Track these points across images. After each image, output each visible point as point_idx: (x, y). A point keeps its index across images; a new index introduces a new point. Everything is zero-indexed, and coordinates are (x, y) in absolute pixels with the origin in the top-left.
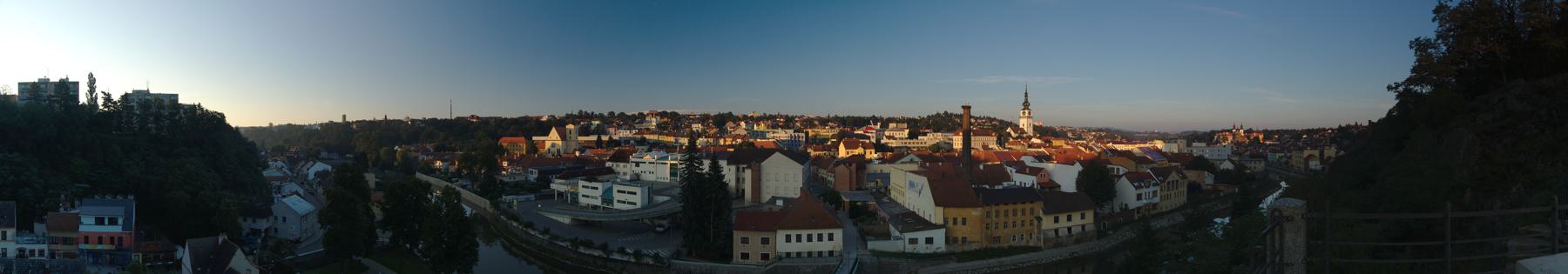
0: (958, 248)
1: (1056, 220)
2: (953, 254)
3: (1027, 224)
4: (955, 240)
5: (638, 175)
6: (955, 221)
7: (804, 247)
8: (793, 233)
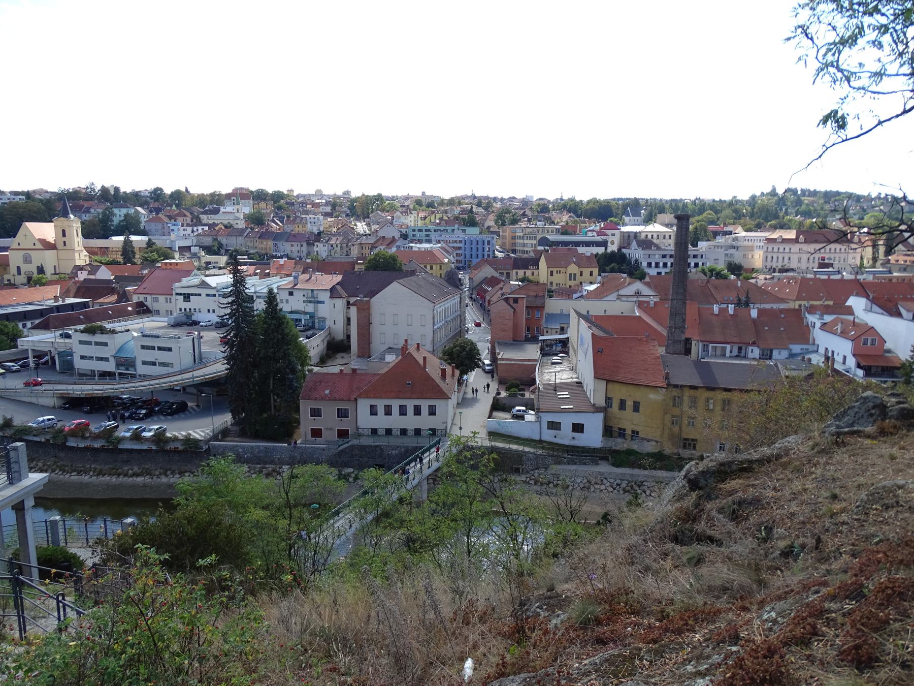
0: (621, 445)
4: (622, 433)
5: (188, 314)
6: (622, 405)
7: (396, 422)
8: (381, 404)
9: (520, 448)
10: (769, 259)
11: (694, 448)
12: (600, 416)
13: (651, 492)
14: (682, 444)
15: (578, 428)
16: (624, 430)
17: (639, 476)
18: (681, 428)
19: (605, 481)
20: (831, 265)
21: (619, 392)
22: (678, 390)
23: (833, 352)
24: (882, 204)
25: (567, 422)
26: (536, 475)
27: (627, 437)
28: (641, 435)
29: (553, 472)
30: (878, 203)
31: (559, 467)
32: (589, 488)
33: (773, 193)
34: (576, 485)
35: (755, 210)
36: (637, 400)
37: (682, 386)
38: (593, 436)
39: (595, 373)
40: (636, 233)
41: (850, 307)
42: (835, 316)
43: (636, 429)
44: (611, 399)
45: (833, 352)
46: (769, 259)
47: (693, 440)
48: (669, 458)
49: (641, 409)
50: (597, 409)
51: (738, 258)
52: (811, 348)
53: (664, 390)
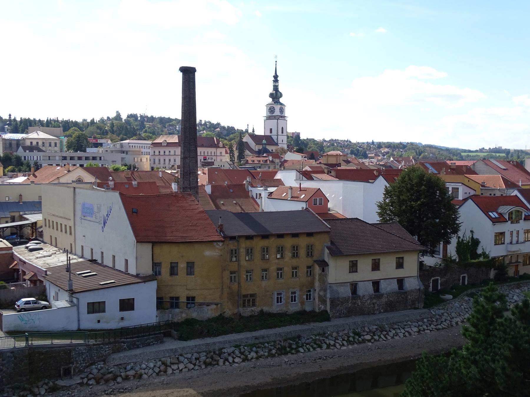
0: (179, 315)
1: (353, 268)
3: (303, 270)
4: (175, 303)
6: (173, 270)
9: (67, 342)
10: (157, 161)
13: (234, 358)
14: (242, 302)
15: (127, 305)
16: (177, 298)
17: (214, 344)
18: (239, 283)
19: (181, 359)
20: (212, 163)
21: (168, 254)
24: (204, 129)
25: (112, 300)
26: (95, 371)
27: (181, 305)
28: (196, 301)
29: (117, 362)
30: (201, 129)
31: (121, 355)
32: (165, 372)
33: (118, 117)
34: (151, 371)
35: (115, 128)
36: (192, 259)
37: (240, 237)
38: (146, 313)
39: (136, 236)
40: (18, 141)
41: (279, 181)
42: (276, 188)
43: (192, 294)
46: (157, 161)
47: (252, 295)
49: (197, 269)
50: (146, 279)
51: (129, 160)
53: (221, 244)
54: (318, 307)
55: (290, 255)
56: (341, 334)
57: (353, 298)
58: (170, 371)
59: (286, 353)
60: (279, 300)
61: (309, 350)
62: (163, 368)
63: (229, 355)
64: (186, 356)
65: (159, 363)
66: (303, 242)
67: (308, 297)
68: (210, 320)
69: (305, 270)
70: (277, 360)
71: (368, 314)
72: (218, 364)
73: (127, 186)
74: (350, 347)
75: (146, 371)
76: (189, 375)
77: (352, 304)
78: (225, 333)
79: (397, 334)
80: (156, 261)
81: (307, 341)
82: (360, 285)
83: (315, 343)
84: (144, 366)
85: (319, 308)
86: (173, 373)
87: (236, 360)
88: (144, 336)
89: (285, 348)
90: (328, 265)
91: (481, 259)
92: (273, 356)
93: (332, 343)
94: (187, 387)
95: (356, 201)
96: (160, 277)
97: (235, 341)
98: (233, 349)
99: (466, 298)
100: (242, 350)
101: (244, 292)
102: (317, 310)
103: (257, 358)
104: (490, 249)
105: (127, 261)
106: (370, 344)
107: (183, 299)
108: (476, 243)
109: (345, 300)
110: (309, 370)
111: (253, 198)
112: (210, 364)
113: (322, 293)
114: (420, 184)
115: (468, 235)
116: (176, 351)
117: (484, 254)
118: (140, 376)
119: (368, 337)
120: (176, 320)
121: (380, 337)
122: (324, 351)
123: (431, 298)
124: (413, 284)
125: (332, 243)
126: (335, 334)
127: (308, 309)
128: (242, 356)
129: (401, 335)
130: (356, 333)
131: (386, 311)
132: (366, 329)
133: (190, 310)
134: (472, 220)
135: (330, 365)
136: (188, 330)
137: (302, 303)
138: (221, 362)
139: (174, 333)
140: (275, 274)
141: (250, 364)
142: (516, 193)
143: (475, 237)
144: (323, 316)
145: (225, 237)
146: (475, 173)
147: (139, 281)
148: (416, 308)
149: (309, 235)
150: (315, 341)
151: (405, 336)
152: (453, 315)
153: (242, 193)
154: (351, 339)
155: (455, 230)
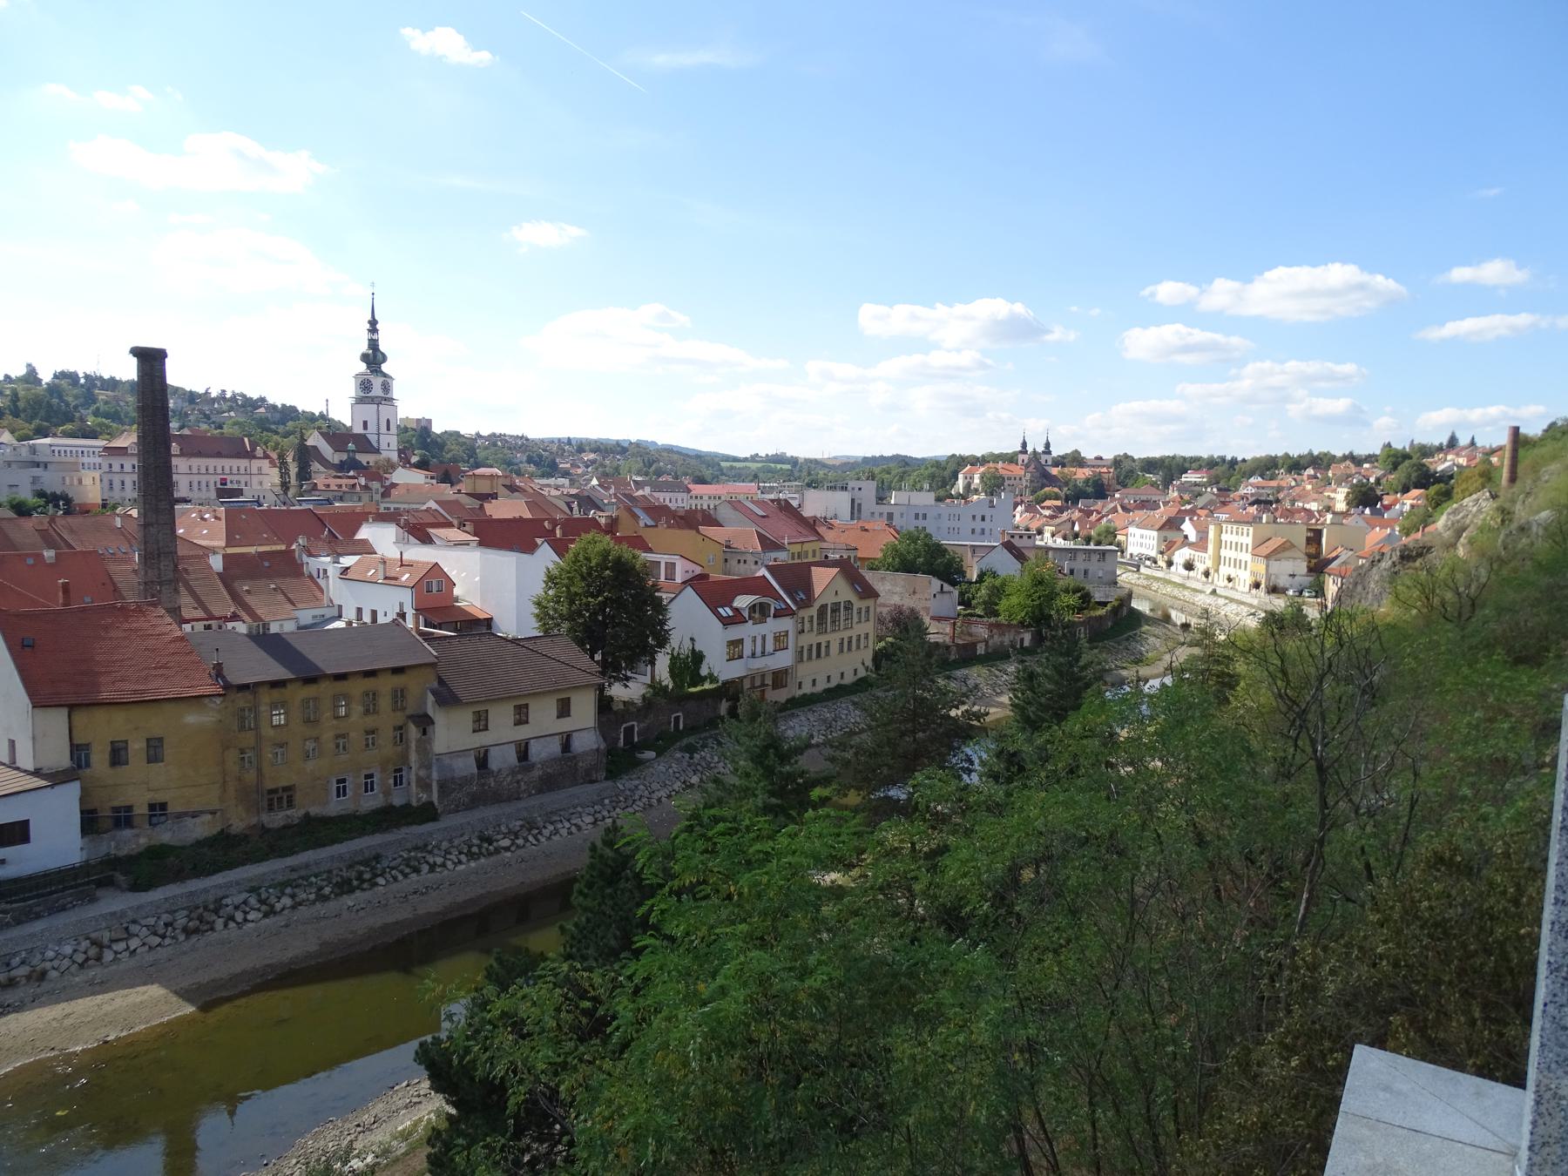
0: (132, 841)
2: (113, 863)
3: (387, 734)
4: (123, 818)
6: (118, 755)
10: (117, 485)
11: (290, 804)
12: (73, 791)
13: (246, 913)
14: (265, 804)
16: (129, 808)
17: (206, 891)
18: (259, 771)
19: (134, 928)
20: (239, 492)
22: (248, 695)
23: (374, 613)
27: (136, 821)
30: (225, 407)
32: (99, 958)
33: (31, 376)
34: (66, 962)
35: (21, 404)
36: (157, 732)
37: (257, 684)
41: (365, 542)
43: (160, 797)
44: (87, 746)
45: (374, 613)
46: (117, 485)
47: (285, 789)
48: (243, 838)
49: (168, 751)
50: (57, 778)
51: (51, 482)
52: (329, 613)
54: (417, 797)
55: (360, 709)
56: (456, 842)
57: (480, 776)
58: (108, 956)
59: (351, 891)
60: (341, 792)
61: (395, 879)
62: (93, 952)
63: (237, 908)
64: (143, 922)
65: (85, 944)
66: (386, 685)
67: (398, 781)
68: (199, 844)
69: (391, 733)
70: (332, 905)
71: (509, 800)
72: (212, 929)
73: (30, 561)
74: (473, 864)
75: (56, 963)
76: (150, 957)
77: (481, 786)
78: (230, 866)
79: (556, 832)
80: (76, 741)
81: (393, 864)
82: (493, 753)
83: (408, 866)
84: (50, 954)
85: (419, 800)
86: (114, 959)
87: (249, 917)
88: (52, 893)
89: (348, 881)
90: (433, 723)
91: (707, 686)
92: (325, 899)
93: (439, 860)
94: (145, 984)
95: (499, 587)
96: (88, 771)
97: (251, 880)
98: (245, 895)
99: (678, 755)
100: (264, 896)
101: (270, 785)
102: (414, 804)
103: (293, 907)
104: (720, 667)
105: (12, 743)
106: (508, 854)
107: (141, 810)
108: (698, 657)
109: (466, 781)
110: (390, 919)
111: (311, 576)
112: (196, 931)
113: (422, 773)
114: (603, 566)
115: (687, 645)
116: (123, 914)
117: (712, 678)
118: (43, 975)
119: (506, 843)
120: (124, 852)
121: (526, 840)
122: (425, 876)
123: (619, 760)
124: (588, 741)
125: (441, 681)
126: (445, 845)
127: (397, 801)
128: (264, 908)
129: (564, 832)
130: (483, 839)
131: (540, 791)
132: (503, 828)
133: (158, 829)
134: (689, 622)
135: (433, 904)
136: (151, 868)
137: (387, 793)
138: (219, 923)
139: (120, 878)
140: (332, 746)
141: (278, 921)
142: (763, 572)
143: (697, 649)
144: (427, 813)
145: (228, 686)
146: (716, 523)
147: (44, 783)
148: (592, 782)
149: (398, 671)
150: (407, 862)
151: (570, 833)
152: (655, 786)
153: (287, 567)
154: (475, 849)
155: (663, 641)
